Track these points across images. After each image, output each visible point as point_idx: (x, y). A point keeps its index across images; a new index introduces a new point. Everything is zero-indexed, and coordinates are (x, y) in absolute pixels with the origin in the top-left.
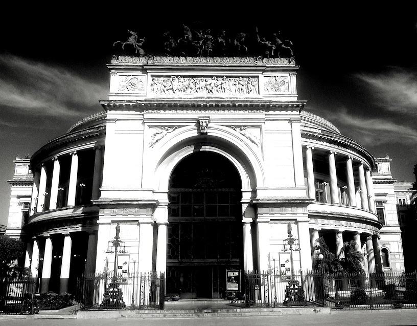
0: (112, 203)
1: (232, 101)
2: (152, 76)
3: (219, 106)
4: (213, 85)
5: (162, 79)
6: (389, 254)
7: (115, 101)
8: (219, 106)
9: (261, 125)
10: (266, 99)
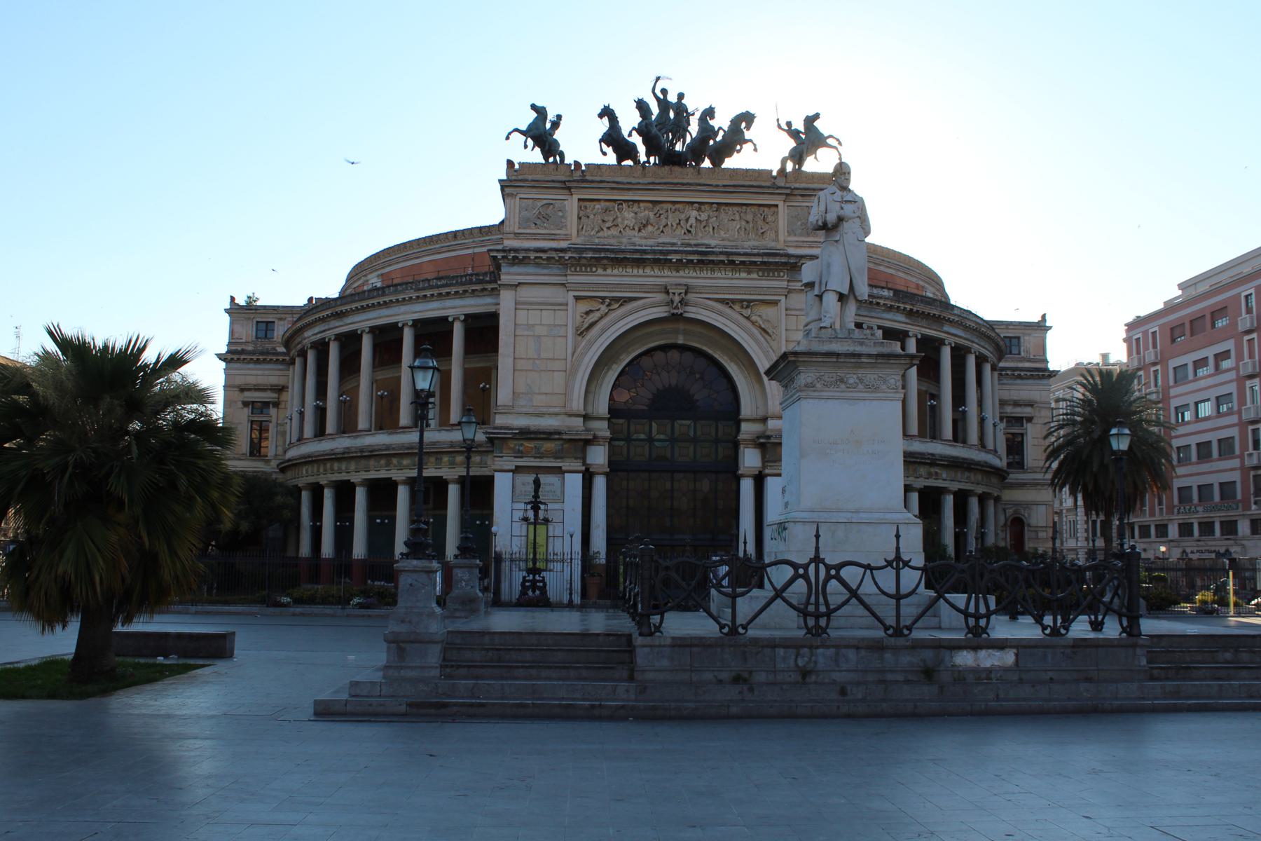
0: (518, 437)
1: (727, 254)
2: (579, 200)
3: (705, 260)
4: (692, 221)
5: (597, 206)
6: (1026, 528)
7: (516, 250)
8: (705, 260)
9: (780, 301)
10: (792, 251)
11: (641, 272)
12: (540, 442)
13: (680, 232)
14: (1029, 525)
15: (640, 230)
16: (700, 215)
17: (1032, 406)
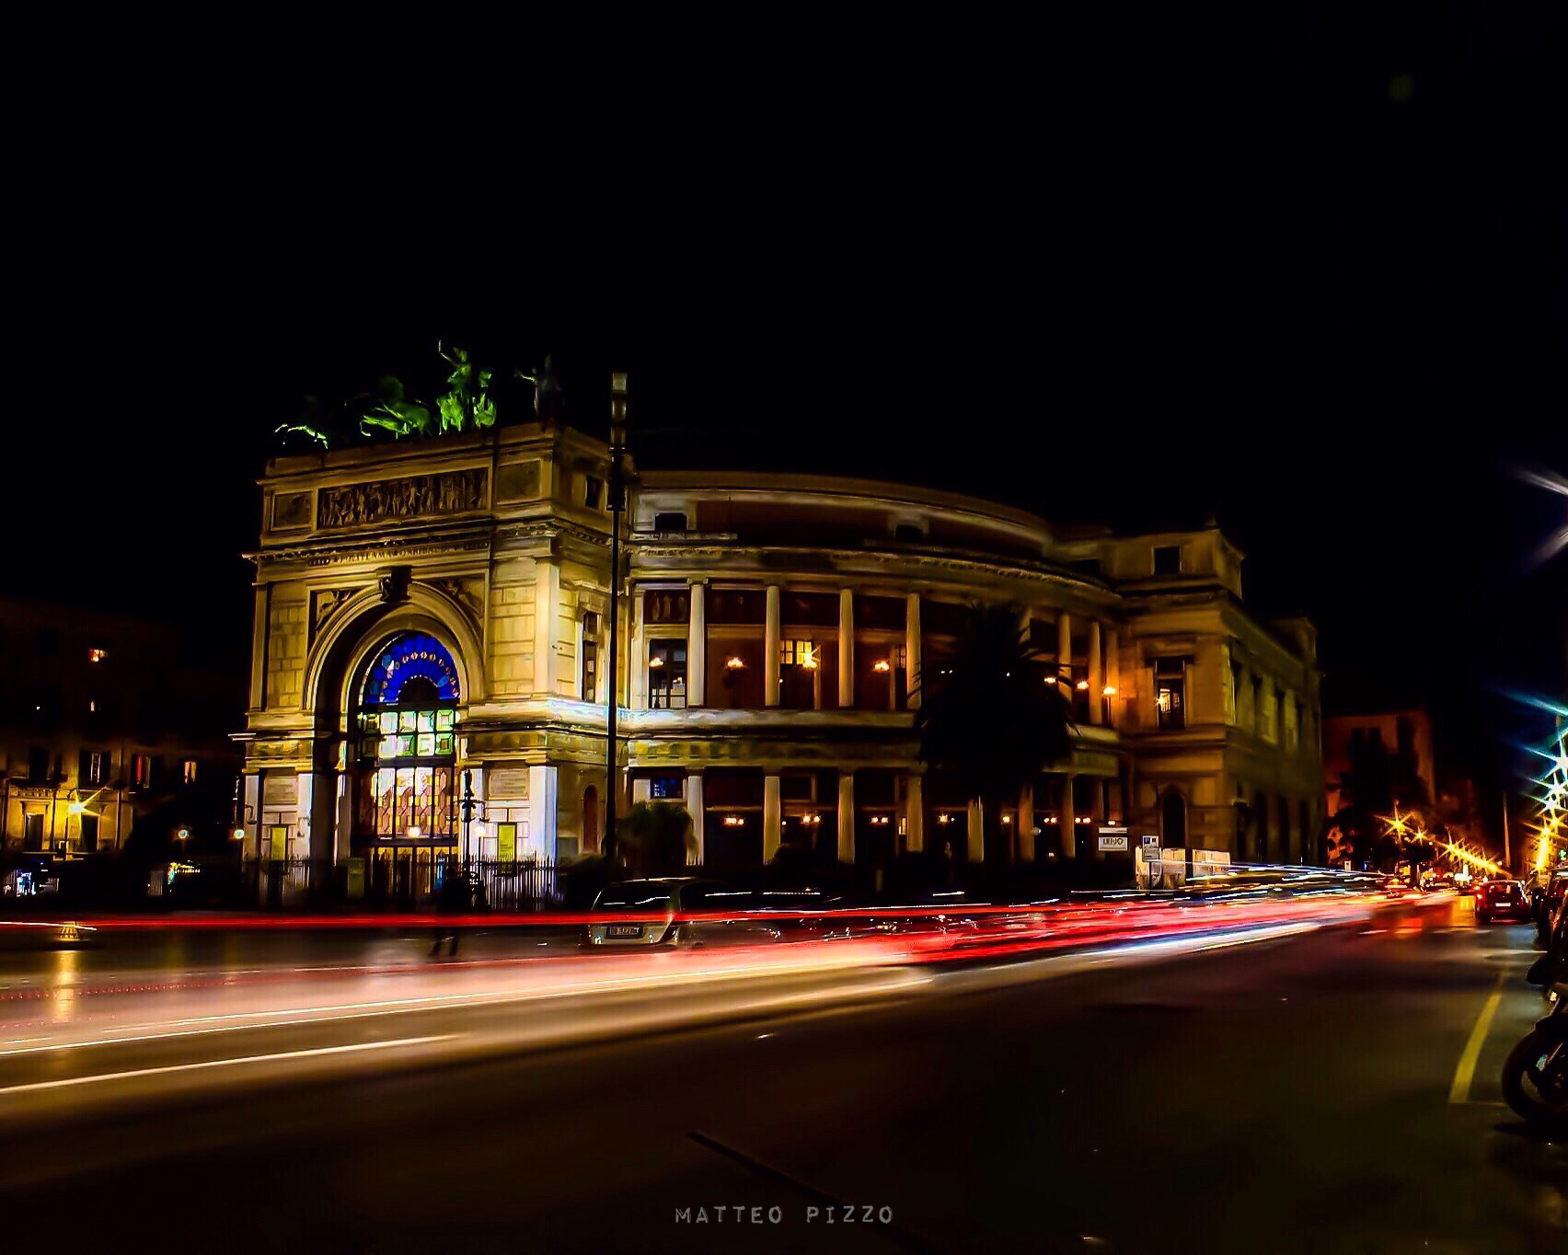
11: (365, 558)
12: (279, 743)
13: (404, 510)
14: (1191, 805)
15: (368, 516)
16: (419, 491)
17: (1193, 641)
